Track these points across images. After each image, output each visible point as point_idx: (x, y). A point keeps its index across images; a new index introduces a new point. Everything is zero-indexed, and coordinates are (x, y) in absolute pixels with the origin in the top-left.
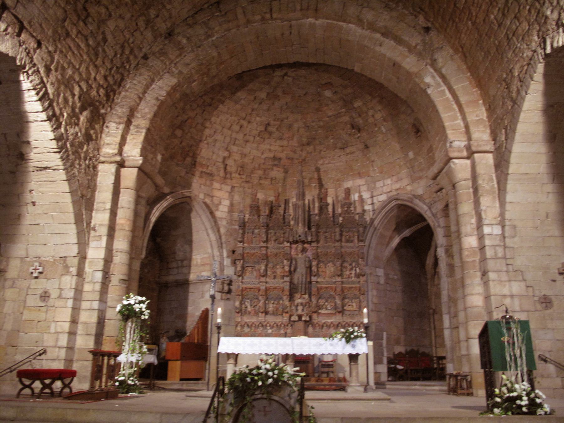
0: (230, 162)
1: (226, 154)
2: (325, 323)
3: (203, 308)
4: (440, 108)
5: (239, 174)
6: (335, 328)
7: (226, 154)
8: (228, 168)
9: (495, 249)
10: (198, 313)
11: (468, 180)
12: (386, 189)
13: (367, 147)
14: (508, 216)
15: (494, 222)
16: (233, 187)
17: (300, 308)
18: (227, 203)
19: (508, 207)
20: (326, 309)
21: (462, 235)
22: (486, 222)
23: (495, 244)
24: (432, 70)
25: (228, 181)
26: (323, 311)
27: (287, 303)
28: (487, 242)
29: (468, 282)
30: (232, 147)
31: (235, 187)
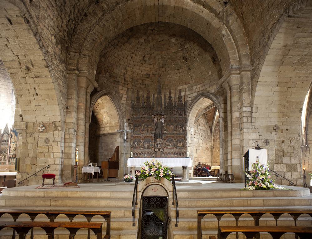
0: (127, 76)
1: (125, 72)
2: (169, 152)
4: (228, 48)
5: (131, 82)
6: (173, 154)
7: (125, 72)
8: (126, 78)
9: (247, 118)
11: (238, 85)
14: (255, 102)
15: (248, 105)
16: (128, 89)
17: (159, 145)
18: (125, 96)
19: (255, 98)
20: (170, 146)
21: (233, 112)
22: (245, 105)
23: (248, 116)
24: (226, 27)
25: (126, 85)
26: (169, 147)
27: (153, 143)
29: (234, 133)
30: (128, 68)
31: (129, 88)
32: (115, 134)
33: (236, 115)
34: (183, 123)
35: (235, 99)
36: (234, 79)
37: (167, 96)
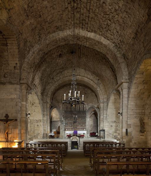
3: (59, 125)
4: (99, 95)
10: (58, 127)
12: (90, 105)
13: (87, 97)
14: (107, 114)
18: (62, 107)
28: (104, 117)
32: (58, 121)
33: (102, 117)
34: (85, 117)
35: (102, 112)
36: (102, 105)
37: (78, 107)
